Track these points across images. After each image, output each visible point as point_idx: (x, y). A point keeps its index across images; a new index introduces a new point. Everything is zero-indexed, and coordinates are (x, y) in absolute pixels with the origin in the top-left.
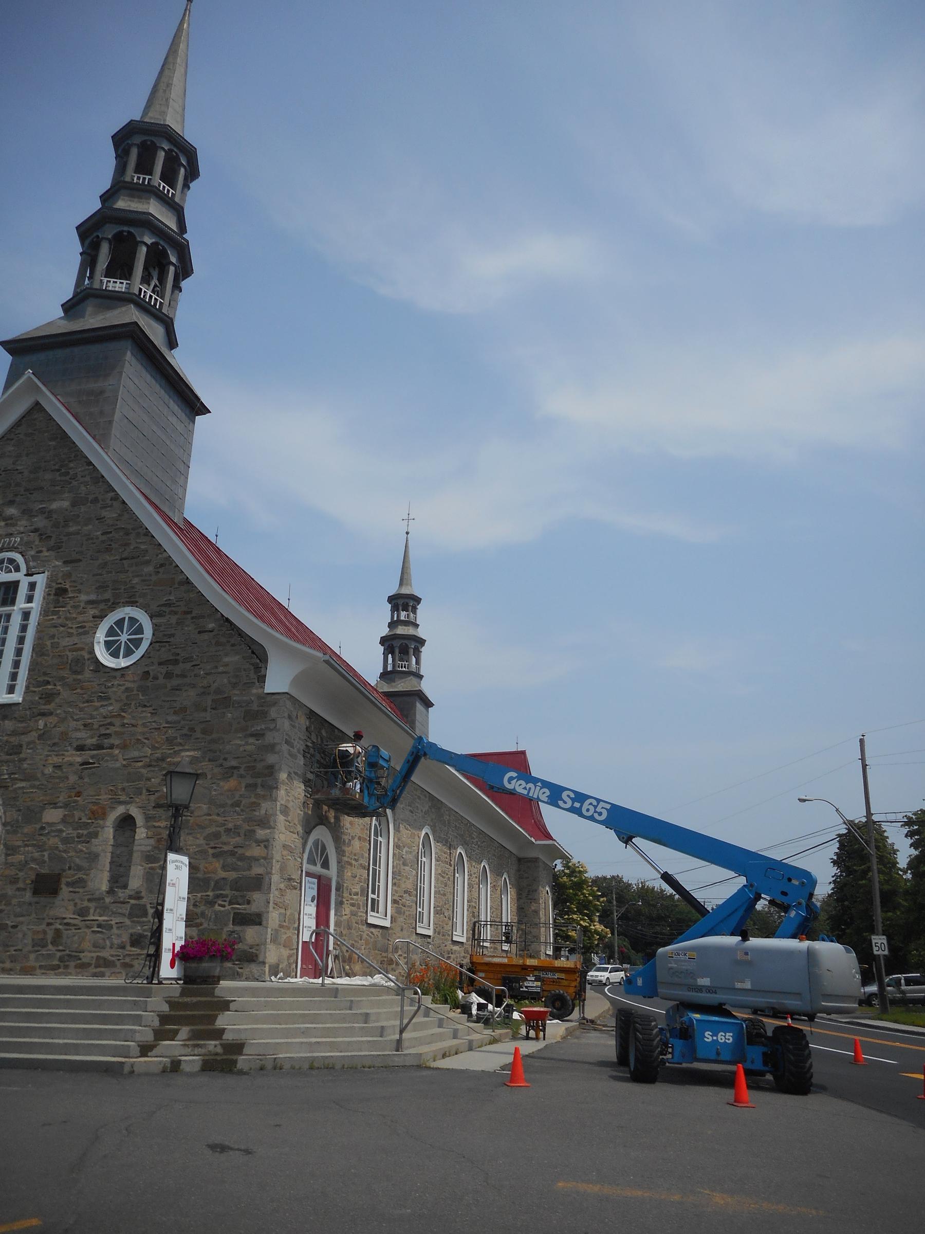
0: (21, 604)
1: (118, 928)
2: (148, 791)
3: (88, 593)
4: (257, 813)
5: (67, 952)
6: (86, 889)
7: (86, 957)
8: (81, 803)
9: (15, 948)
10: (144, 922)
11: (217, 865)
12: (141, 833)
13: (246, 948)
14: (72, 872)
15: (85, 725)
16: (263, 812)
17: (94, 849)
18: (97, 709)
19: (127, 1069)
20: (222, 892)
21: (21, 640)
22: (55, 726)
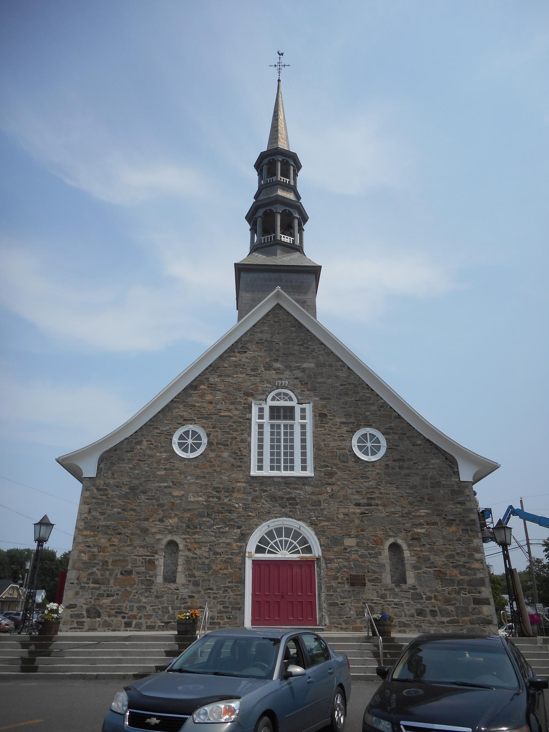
0: (298, 420)
1: (407, 605)
2: (405, 530)
3: (340, 418)
8: (366, 535)
9: (346, 616)
10: (422, 603)
11: (456, 572)
12: (407, 554)
14: (370, 574)
15: (357, 492)
16: (475, 544)
17: (380, 561)
18: (362, 483)
22: (339, 491)
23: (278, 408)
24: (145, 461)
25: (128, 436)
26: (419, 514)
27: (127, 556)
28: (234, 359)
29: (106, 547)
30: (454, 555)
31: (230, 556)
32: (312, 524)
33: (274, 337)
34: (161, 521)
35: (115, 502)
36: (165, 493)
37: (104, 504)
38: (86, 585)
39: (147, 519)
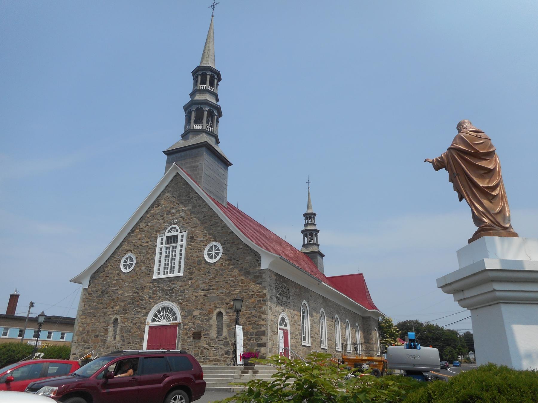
0: (179, 242)
4: (262, 310)
5: (205, 357)
6: (209, 336)
7: (212, 358)
8: (205, 308)
10: (228, 347)
12: (225, 317)
13: (262, 354)
14: (204, 331)
15: (204, 282)
16: (263, 309)
17: (210, 323)
18: (207, 277)
19: (232, 390)
20: (252, 336)
21: (181, 255)
23: (171, 237)
24: (108, 276)
25: (102, 263)
26: (235, 293)
27: (97, 328)
28: (153, 211)
29: (89, 324)
30: (250, 317)
31: (140, 325)
32: (180, 304)
33: (174, 194)
34: (112, 308)
35: (95, 300)
36: (116, 293)
37: (90, 301)
38: (80, 343)
39: (106, 308)
